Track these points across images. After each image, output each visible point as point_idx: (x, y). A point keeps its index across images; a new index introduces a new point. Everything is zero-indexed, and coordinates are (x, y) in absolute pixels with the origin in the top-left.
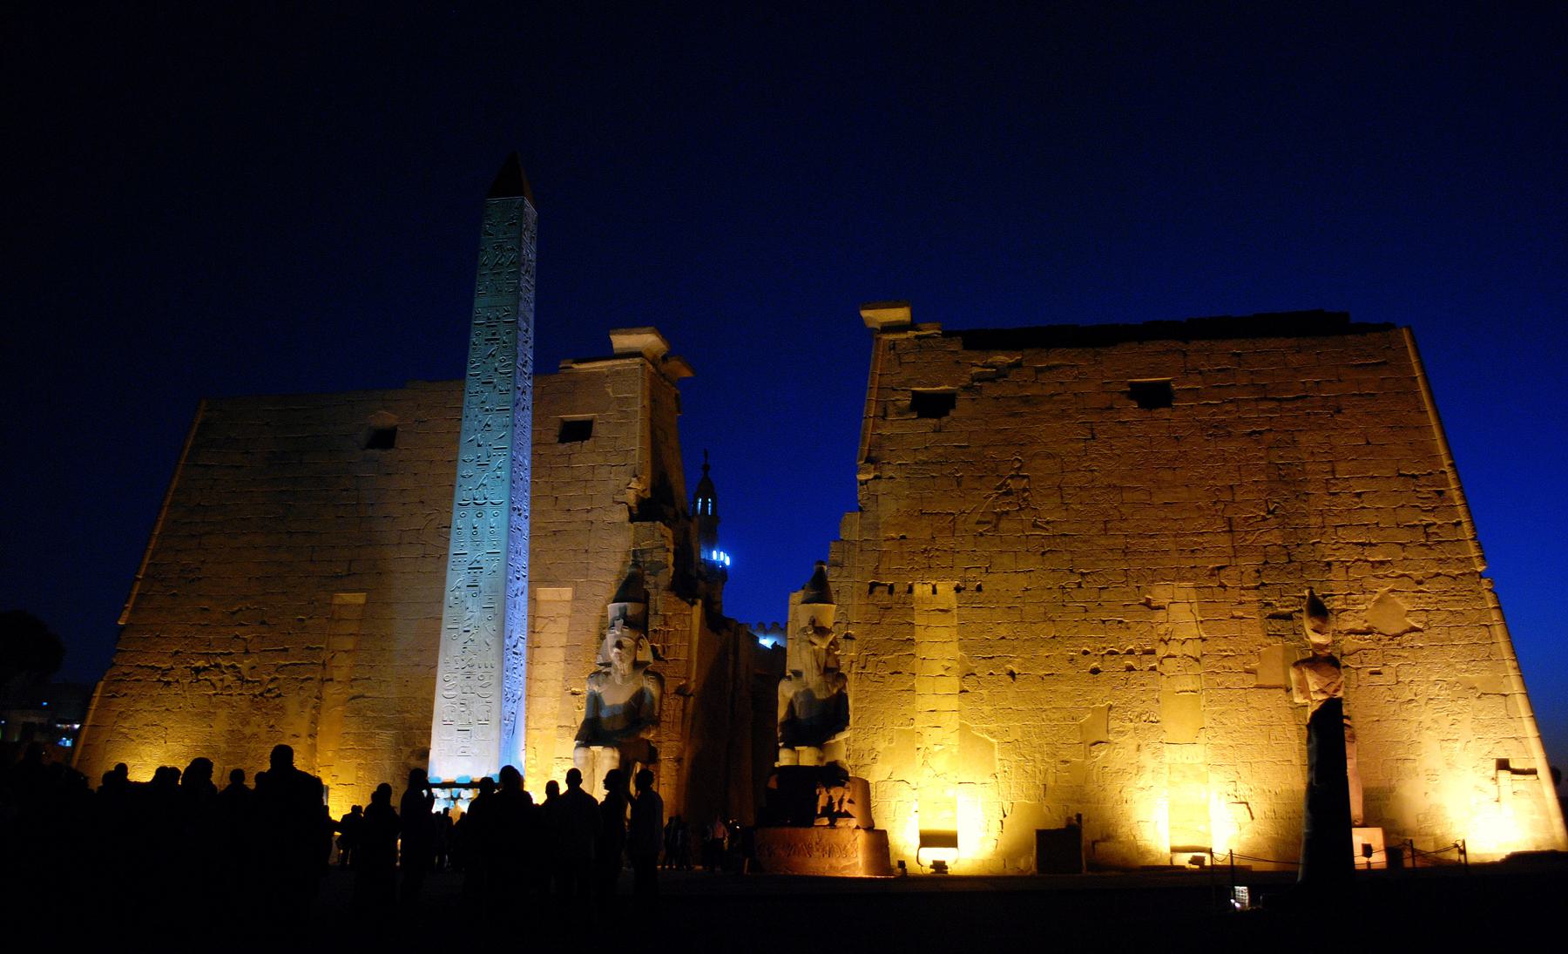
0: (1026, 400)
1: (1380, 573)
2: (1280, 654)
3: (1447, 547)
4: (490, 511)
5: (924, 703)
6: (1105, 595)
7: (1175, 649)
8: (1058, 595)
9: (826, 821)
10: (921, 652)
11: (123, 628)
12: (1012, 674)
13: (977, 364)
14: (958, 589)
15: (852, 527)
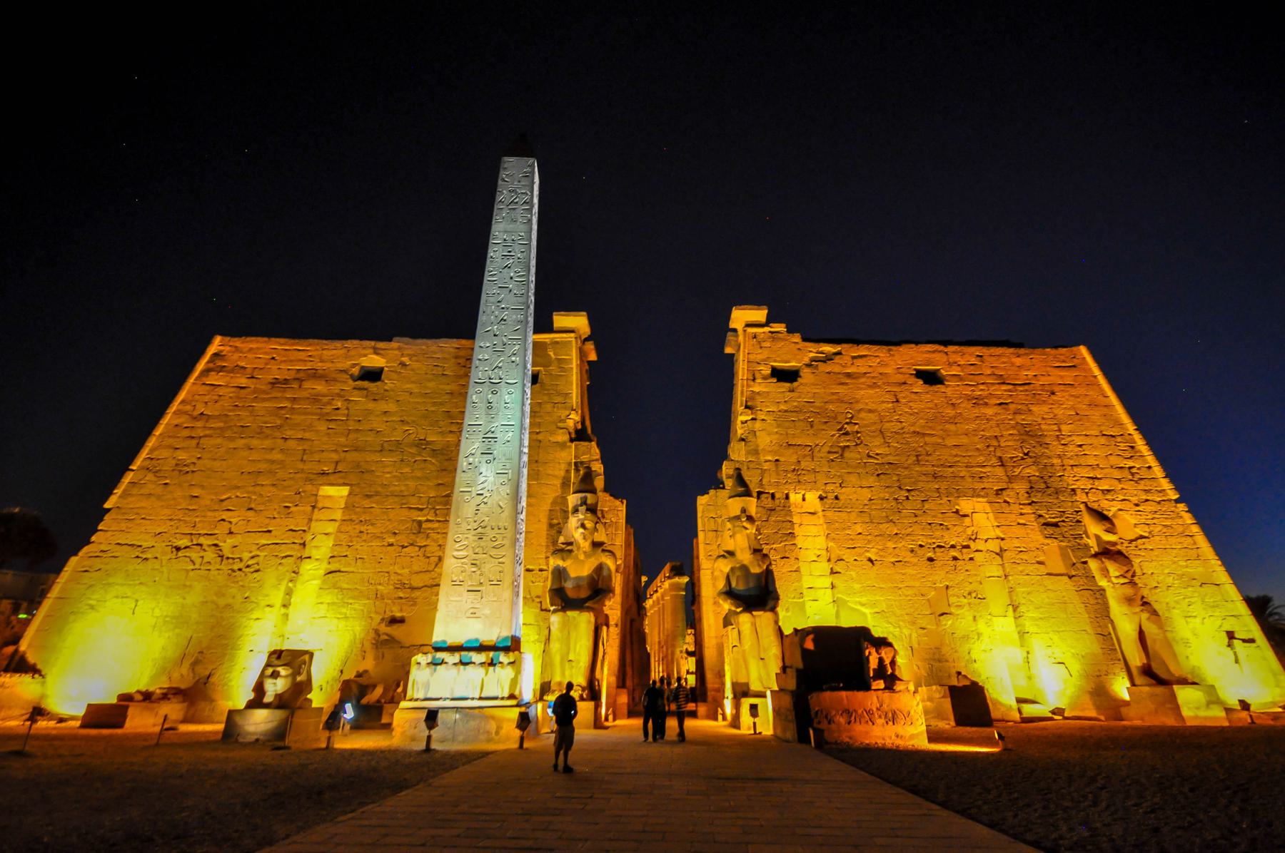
0: (849, 375)
1: (1109, 497)
2: (1057, 550)
3: (1148, 482)
4: (504, 389)
5: (807, 581)
6: (927, 506)
7: (980, 545)
8: (894, 503)
9: (880, 684)
10: (799, 541)
11: (108, 510)
12: (870, 560)
13: (813, 350)
14: (821, 498)
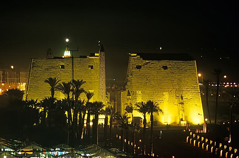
7: (165, 100)
15: (129, 83)
